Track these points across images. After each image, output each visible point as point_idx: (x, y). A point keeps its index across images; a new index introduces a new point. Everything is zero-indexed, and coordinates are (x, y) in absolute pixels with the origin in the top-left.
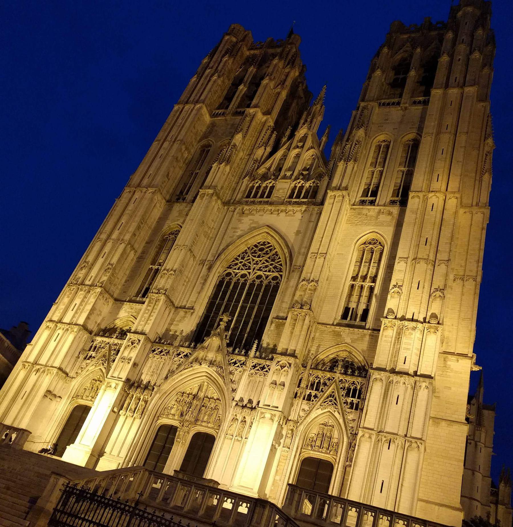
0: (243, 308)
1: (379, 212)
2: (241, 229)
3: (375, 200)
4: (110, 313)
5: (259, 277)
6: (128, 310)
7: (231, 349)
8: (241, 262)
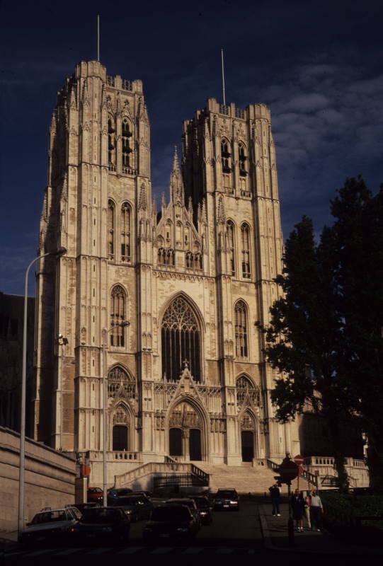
5: (184, 327)
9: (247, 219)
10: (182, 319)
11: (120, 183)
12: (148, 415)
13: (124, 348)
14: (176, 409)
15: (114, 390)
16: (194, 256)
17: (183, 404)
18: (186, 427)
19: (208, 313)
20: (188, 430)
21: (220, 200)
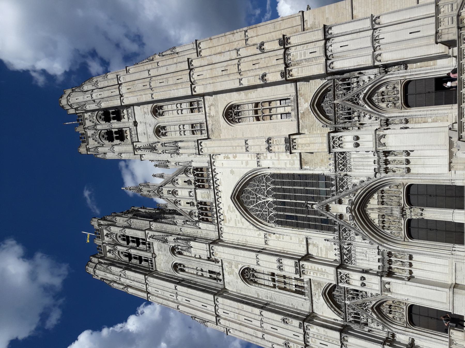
0: (296, 198)
1: (209, 116)
5: (268, 193)
8: (260, 211)
11: (159, 254)
12: (387, 286)
15: (359, 314)
16: (197, 178)
17: (369, 212)
18: (403, 214)
19: (247, 163)
21: (139, 149)
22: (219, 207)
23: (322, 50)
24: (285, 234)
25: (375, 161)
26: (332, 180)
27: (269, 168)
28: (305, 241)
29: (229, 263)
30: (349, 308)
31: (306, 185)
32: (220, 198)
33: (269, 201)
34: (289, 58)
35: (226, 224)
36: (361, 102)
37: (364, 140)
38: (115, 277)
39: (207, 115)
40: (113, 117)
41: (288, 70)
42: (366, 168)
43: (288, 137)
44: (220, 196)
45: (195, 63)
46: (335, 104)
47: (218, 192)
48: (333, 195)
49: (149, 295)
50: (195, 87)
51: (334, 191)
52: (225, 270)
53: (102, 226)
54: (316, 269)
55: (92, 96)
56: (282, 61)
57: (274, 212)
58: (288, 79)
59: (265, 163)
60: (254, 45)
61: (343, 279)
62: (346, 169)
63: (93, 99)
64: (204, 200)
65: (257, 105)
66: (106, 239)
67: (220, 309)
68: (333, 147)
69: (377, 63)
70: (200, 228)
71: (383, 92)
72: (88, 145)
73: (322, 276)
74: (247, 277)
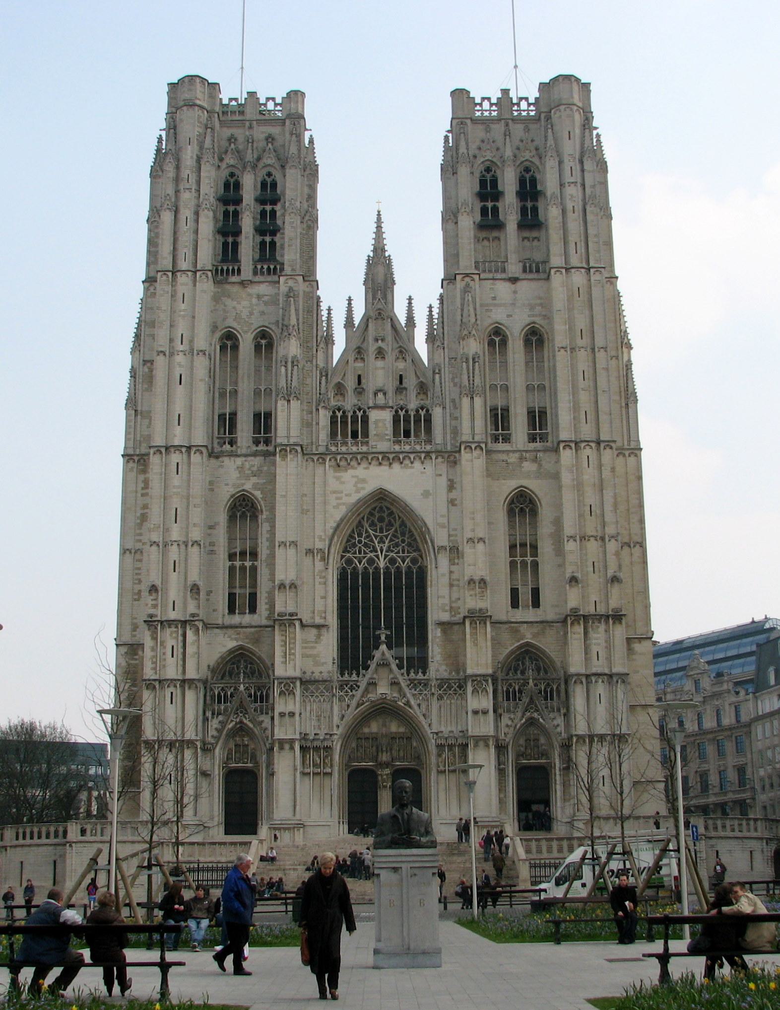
0: (388, 608)
1: (522, 459)
2: (345, 492)
3: (510, 435)
4: (209, 644)
5: (393, 561)
6: (233, 636)
7: (404, 671)
8: (360, 542)
9: (537, 319)
10: (386, 544)
11: (250, 295)
12: (287, 746)
13: (256, 616)
14: (366, 730)
16: (412, 414)
19: (443, 526)
20: (387, 771)
22: (362, 459)
23: (599, 670)
24: (330, 587)
25: (453, 732)
26: (424, 673)
27: (436, 567)
28: (322, 622)
29: (260, 470)
30: (232, 689)
31: (410, 627)
32: (377, 463)
33: (379, 559)
34: (595, 621)
35: (331, 473)
36: (528, 714)
37: (482, 720)
38: (188, 172)
39: (524, 454)
40: (527, 208)
41: (580, 619)
42: (442, 719)
43: (489, 614)
44: (384, 463)
45: (607, 455)
46: (528, 679)
47: (389, 459)
48: (402, 674)
49: (170, 274)
50: (571, 448)
51: (408, 675)
52: (246, 461)
53: (294, 136)
54: (291, 646)
55: (573, 183)
56: (592, 611)
57: (360, 567)
58: (569, 618)
59: (443, 560)
60: (620, 567)
61: (284, 686)
62: (440, 694)
63: (567, 185)
64: (371, 426)
65: (534, 547)
66: (260, 133)
67: (180, 455)
68: (473, 681)
69: (575, 739)
70: (317, 410)
71: (538, 740)
72: (471, 119)
73: (283, 654)
74: (238, 504)
